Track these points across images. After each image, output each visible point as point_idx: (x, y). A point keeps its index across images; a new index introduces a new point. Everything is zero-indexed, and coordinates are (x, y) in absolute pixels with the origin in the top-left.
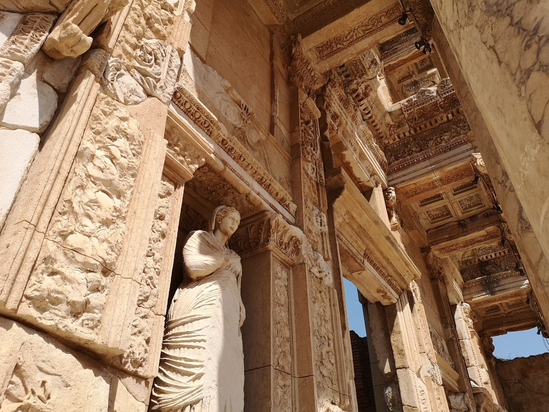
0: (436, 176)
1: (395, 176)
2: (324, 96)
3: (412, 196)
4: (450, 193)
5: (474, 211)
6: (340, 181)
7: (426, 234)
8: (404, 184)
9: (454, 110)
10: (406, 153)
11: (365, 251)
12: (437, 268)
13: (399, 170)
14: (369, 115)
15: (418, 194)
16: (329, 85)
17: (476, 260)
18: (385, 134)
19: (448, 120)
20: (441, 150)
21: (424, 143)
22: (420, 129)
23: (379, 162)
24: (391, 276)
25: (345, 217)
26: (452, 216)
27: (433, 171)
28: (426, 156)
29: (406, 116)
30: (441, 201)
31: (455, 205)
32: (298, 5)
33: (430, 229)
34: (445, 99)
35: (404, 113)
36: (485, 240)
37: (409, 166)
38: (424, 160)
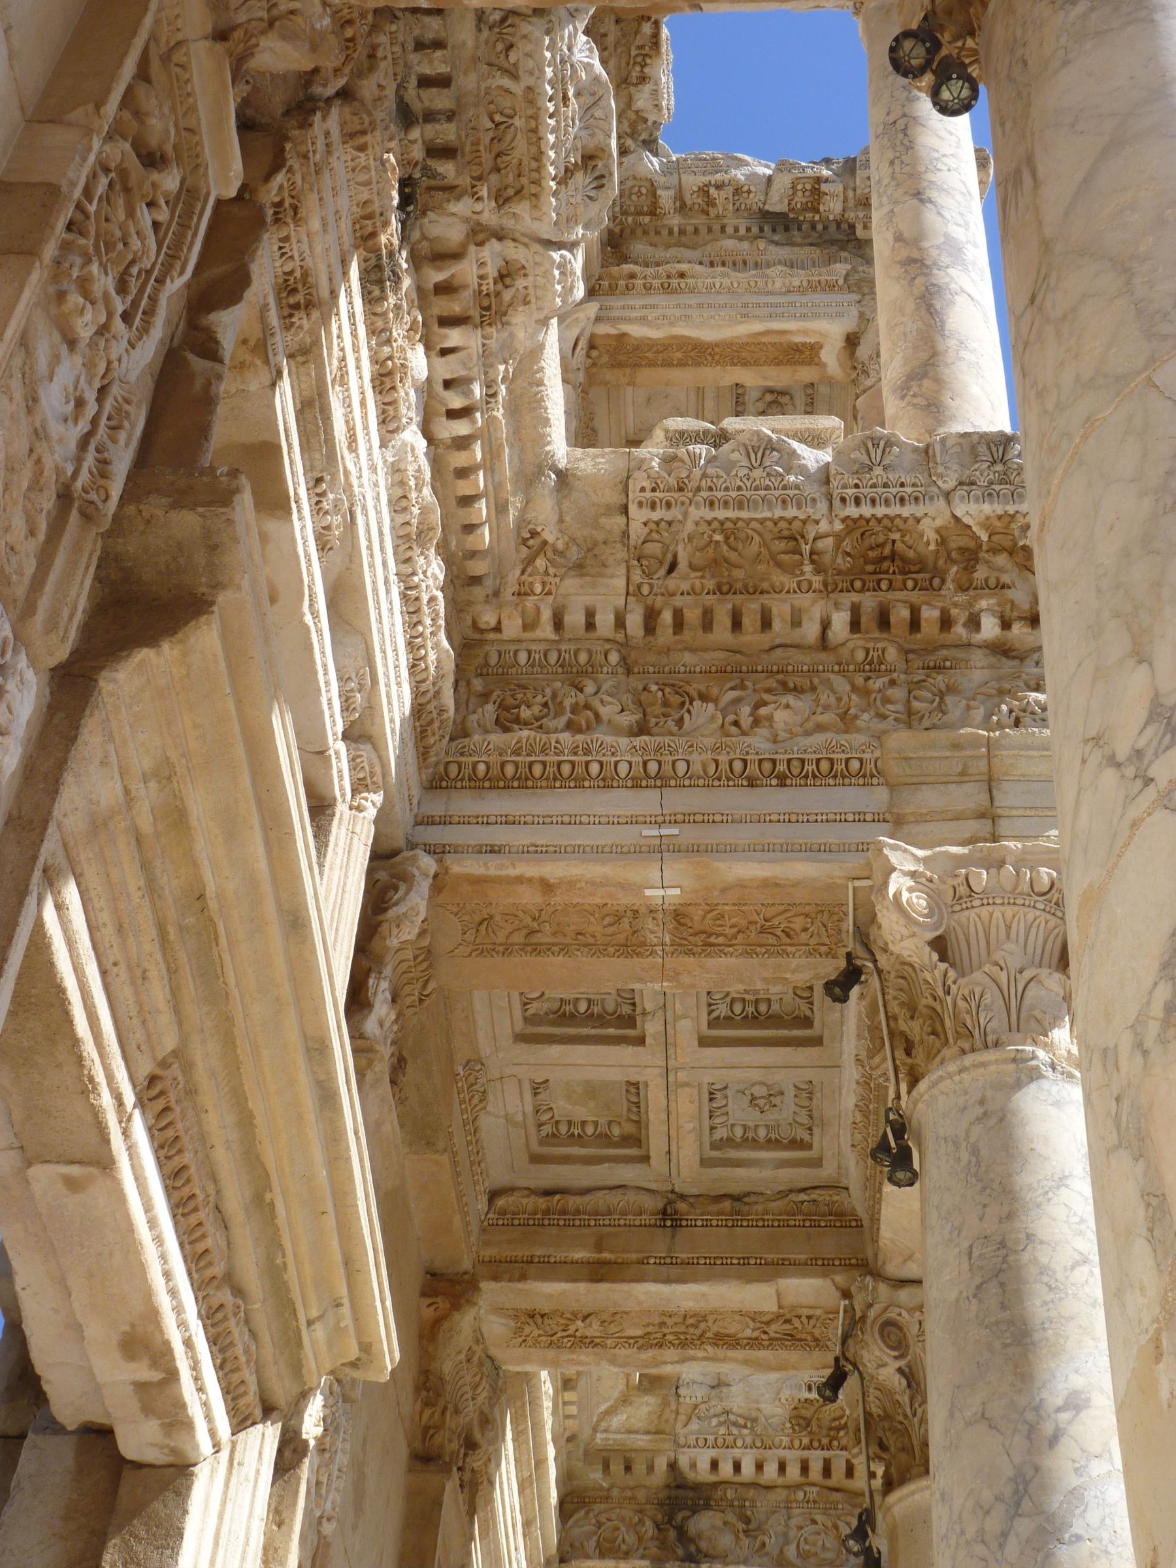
0: (664, 886)
1: (465, 804)
2: (287, 138)
4: (685, 1025)
5: (762, 1173)
6: (200, 558)
7: (482, 1205)
8: (490, 867)
9: (869, 602)
10: (560, 712)
11: (164, 1064)
12: (470, 1412)
13: (495, 781)
14: (461, 428)
15: (538, 950)
16: (335, 112)
17: (661, 1464)
18: (501, 575)
19: (823, 642)
21: (666, 704)
23: (417, 694)
24: (238, 1292)
25: (137, 787)
26: (646, 1159)
27: (660, 850)
28: (653, 767)
29: (637, 530)
30: (626, 1053)
31: (687, 1105)
34: (849, 531)
35: (633, 509)
36: (754, 1343)
37: (555, 779)
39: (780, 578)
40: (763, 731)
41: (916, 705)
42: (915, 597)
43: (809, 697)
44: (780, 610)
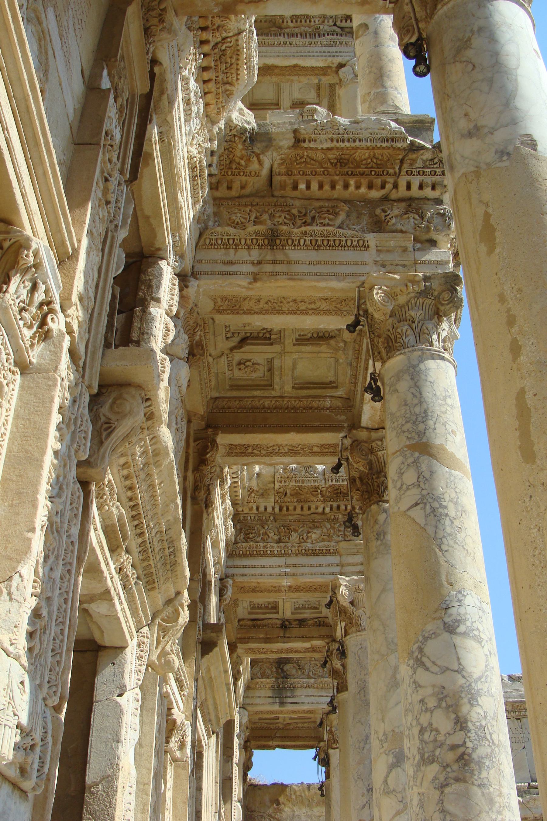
0: (286, 582)
1: (238, 562)
3: (248, 592)
5: (307, 614)
7: (237, 624)
8: (246, 579)
9: (335, 505)
10: (259, 535)
13: (245, 555)
19: (323, 513)
20: (303, 551)
21: (285, 532)
22: (288, 509)
26: (278, 613)
28: (283, 552)
32: (227, 387)
33: (243, 620)
35: (276, 482)
37: (259, 555)
38: (279, 555)
39: (312, 498)
40: (309, 541)
41: (346, 533)
42: (346, 503)
43: (320, 529)
44: (313, 506)
